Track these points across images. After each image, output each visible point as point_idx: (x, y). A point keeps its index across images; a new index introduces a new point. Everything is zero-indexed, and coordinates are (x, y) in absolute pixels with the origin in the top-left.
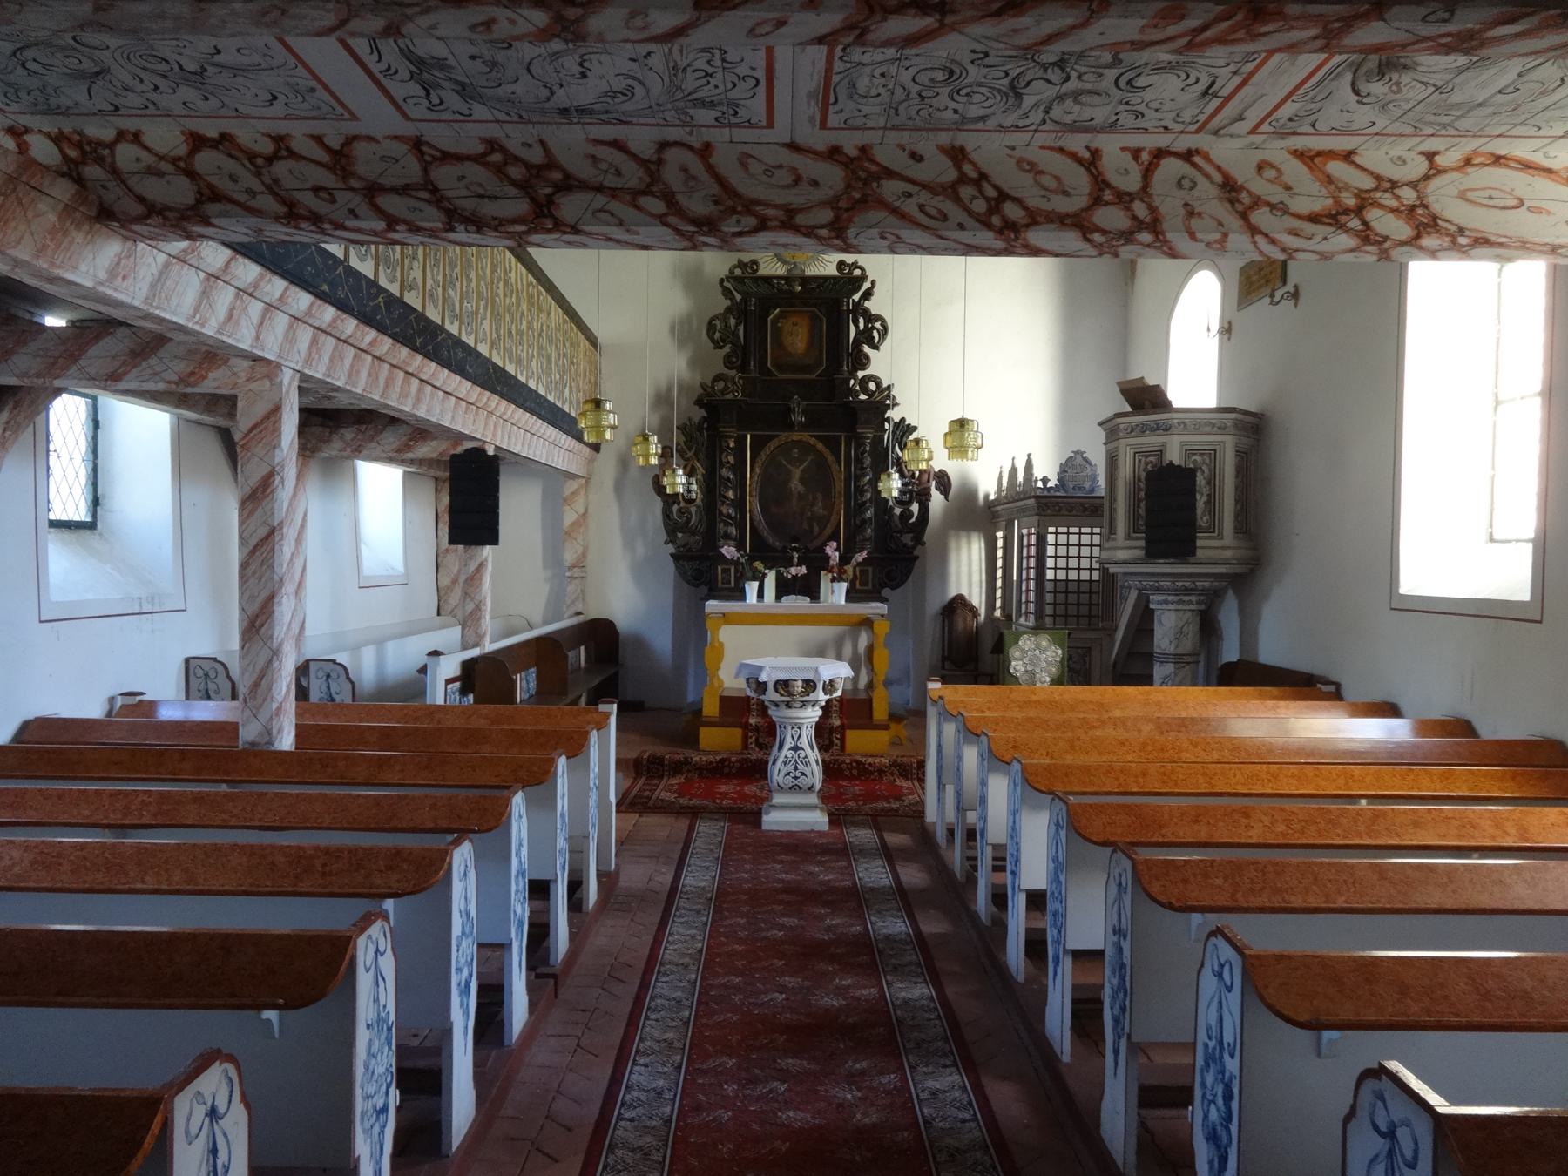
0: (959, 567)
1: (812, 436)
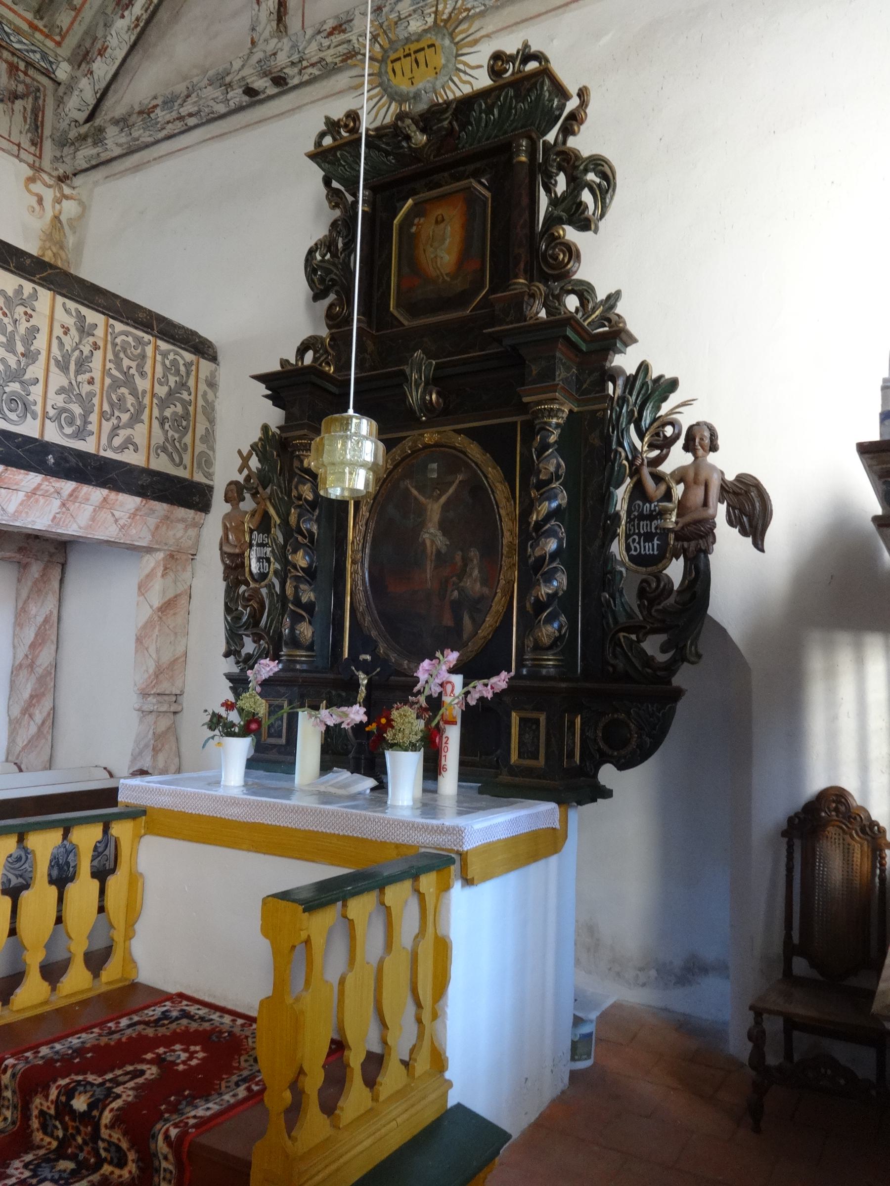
0: (833, 719)
1: (458, 432)
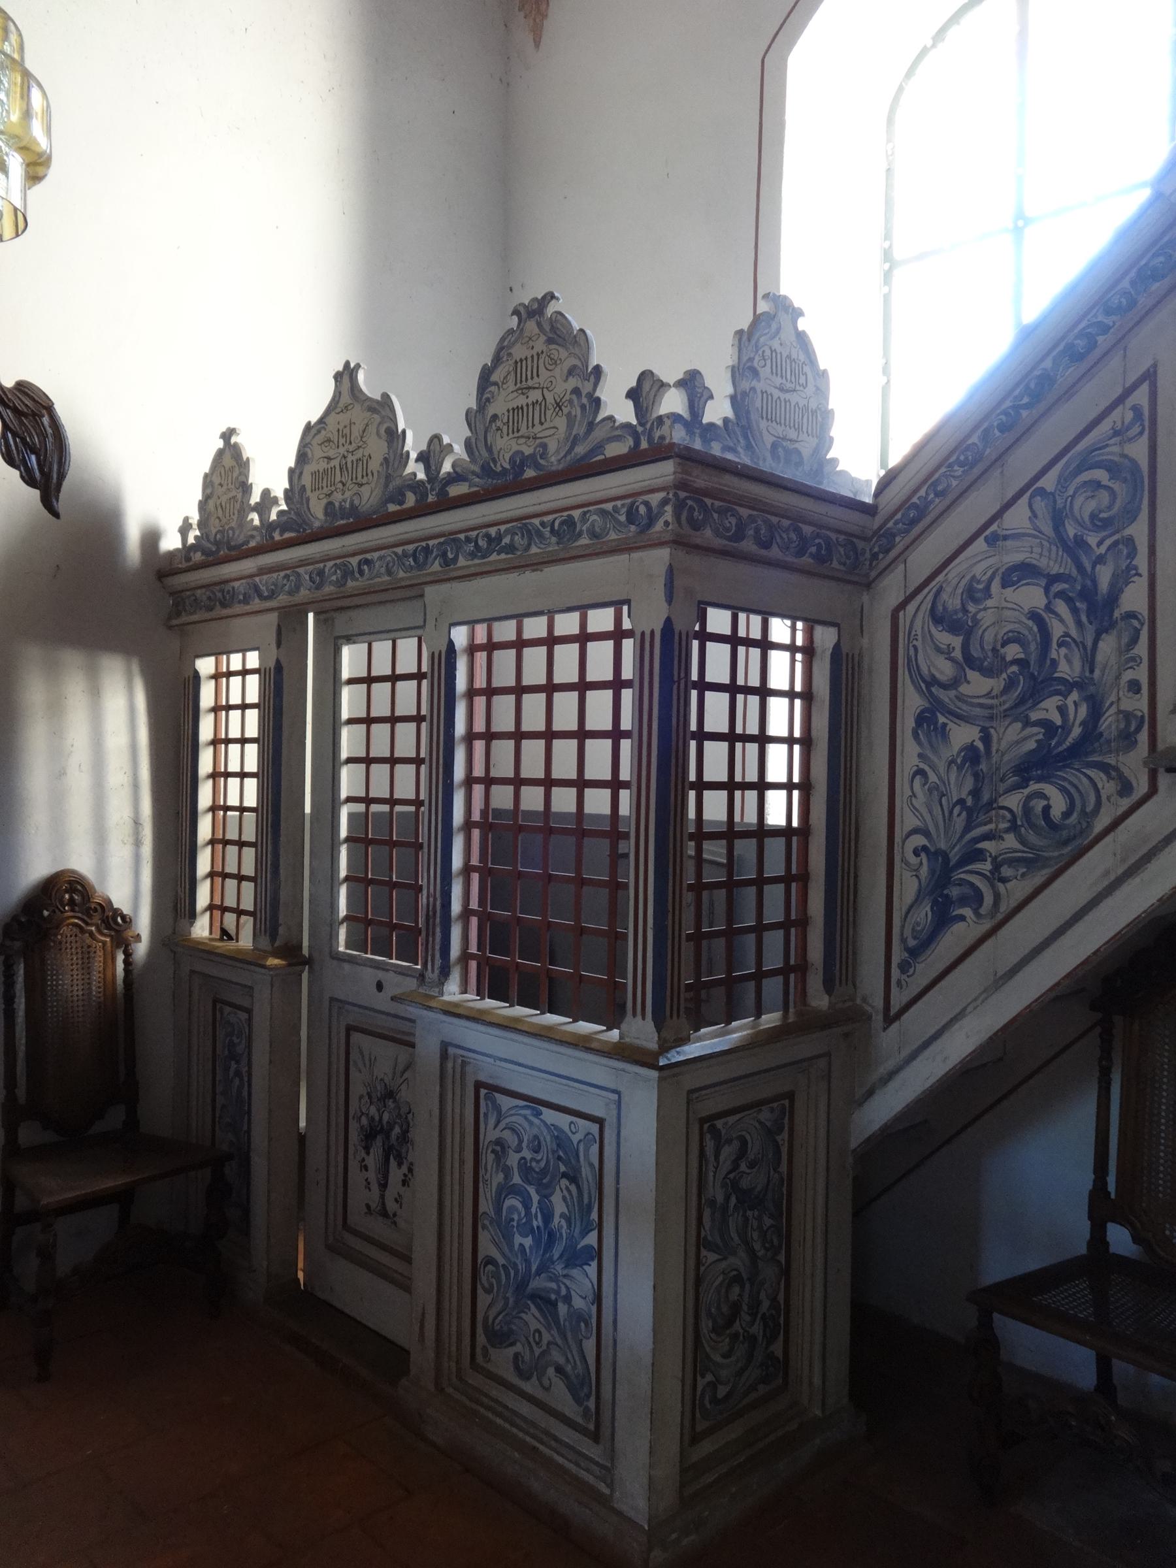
0: (60, 774)
